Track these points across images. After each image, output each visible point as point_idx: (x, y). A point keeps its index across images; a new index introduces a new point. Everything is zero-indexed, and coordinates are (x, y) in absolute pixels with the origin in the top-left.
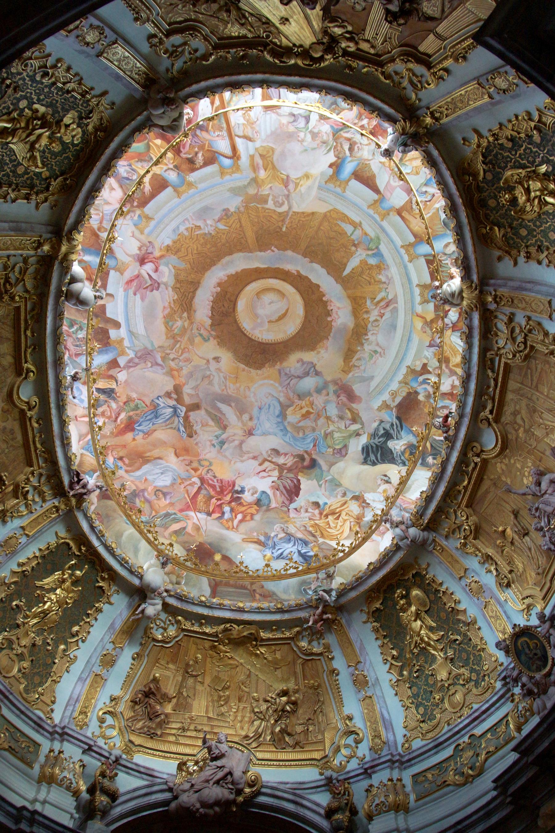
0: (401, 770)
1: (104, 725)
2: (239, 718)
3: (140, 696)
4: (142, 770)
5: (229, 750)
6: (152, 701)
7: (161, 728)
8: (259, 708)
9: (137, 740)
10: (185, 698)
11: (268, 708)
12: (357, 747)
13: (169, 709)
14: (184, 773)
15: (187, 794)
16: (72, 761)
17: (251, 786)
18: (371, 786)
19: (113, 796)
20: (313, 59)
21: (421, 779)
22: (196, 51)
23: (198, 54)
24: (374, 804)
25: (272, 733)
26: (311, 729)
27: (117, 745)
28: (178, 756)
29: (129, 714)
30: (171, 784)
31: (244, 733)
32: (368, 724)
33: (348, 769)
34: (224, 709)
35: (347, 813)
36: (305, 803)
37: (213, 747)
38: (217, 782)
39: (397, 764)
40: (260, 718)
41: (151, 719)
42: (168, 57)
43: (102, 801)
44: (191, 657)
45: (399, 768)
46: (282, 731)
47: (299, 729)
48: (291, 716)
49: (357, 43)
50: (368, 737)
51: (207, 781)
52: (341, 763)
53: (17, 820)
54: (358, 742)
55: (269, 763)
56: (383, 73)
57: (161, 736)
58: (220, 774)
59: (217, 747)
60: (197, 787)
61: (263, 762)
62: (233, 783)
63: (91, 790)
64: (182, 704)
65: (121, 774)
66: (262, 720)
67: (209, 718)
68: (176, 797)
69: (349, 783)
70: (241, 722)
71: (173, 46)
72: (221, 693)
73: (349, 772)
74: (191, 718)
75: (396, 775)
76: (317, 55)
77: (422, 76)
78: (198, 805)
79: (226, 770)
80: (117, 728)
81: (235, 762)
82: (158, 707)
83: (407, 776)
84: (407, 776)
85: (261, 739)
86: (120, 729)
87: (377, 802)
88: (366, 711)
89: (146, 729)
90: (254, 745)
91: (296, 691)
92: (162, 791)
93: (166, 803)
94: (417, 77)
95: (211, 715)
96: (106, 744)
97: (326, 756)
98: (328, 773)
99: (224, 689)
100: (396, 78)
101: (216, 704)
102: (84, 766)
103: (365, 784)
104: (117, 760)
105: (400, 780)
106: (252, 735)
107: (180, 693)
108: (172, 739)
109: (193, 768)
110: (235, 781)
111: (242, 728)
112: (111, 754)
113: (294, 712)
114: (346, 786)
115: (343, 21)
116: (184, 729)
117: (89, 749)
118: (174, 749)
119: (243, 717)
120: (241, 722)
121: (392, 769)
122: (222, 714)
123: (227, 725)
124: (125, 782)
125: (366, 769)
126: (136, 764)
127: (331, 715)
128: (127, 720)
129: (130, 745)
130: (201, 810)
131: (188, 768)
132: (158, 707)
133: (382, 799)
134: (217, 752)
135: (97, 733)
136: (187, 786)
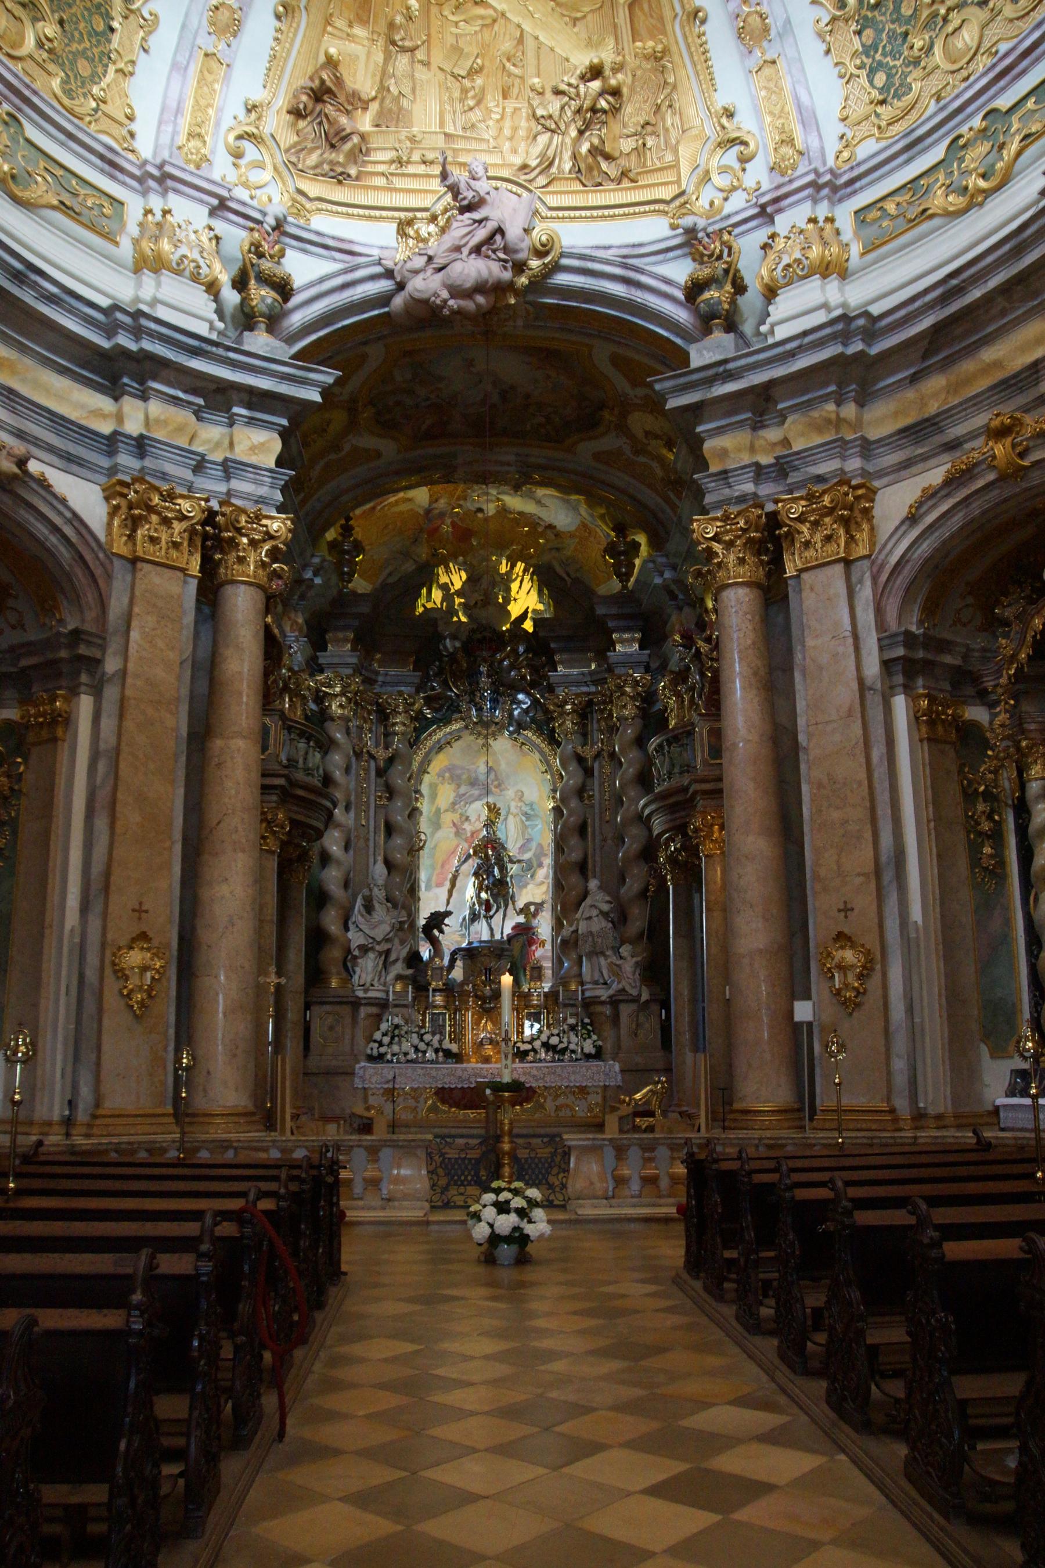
0: (832, 204)
1: (242, 162)
2: (507, 132)
3: (304, 98)
4: (331, 243)
5: (493, 192)
6: (329, 109)
7: (355, 163)
8: (545, 108)
9: (314, 189)
10: (396, 100)
11: (562, 108)
12: (744, 170)
13: (365, 122)
14: (411, 242)
15: (421, 276)
16: (191, 228)
17: (540, 254)
18: (773, 236)
19: (284, 288)
21: (874, 214)
24: (780, 267)
25: (574, 157)
26: (649, 144)
27: (276, 199)
28: (396, 214)
29: (287, 138)
30: (389, 264)
31: (518, 161)
32: (768, 119)
33: (725, 212)
34: (476, 116)
35: (728, 287)
36: (644, 279)
37: (463, 186)
38: (477, 250)
39: (825, 191)
40: (548, 129)
41: (333, 146)
43: (263, 299)
44: (398, 7)
45: (829, 199)
46: (596, 151)
47: (627, 145)
48: (610, 119)
50: (765, 146)
51: (458, 249)
52: (712, 204)
53: (110, 331)
54: (744, 160)
55: (572, 213)
57: (357, 178)
58: (481, 234)
59: (469, 187)
60: (439, 261)
61: (561, 214)
62: (506, 249)
63: (240, 283)
64: (390, 110)
65: (289, 252)
66: (553, 131)
67: (446, 135)
68: (401, 286)
69: (730, 233)
70: (511, 139)
72: (467, 83)
73: (729, 216)
74: (412, 139)
75: (822, 211)
78: (445, 294)
79: (491, 226)
80: (269, 167)
81: (508, 210)
82: (343, 120)
83: (845, 215)
84: (845, 215)
85: (554, 170)
86: (275, 169)
87: (786, 260)
88: (763, 93)
89: (326, 167)
90: (542, 181)
91: (618, 68)
92: (373, 278)
93: (384, 299)
95: (450, 129)
96: (252, 198)
97: (683, 193)
98: (688, 221)
99: (472, 73)
101: (458, 107)
102: (218, 238)
103: (761, 235)
104: (279, 226)
105: (830, 220)
106: (534, 163)
107: (383, 89)
108: (381, 181)
109: (426, 229)
110: (511, 245)
111: (515, 151)
112: (265, 214)
113: (615, 110)
114: (726, 237)
116: (400, 162)
117: (221, 207)
118: (385, 200)
119: (515, 129)
120: (511, 139)
121: (815, 201)
122: (473, 126)
123: (484, 146)
124: (301, 268)
125: (763, 207)
126: (318, 233)
127: (691, 111)
128: (287, 151)
129: (300, 198)
130: (451, 302)
131: (417, 232)
132: (343, 120)
133: (797, 255)
134: (470, 195)
135: (232, 176)
136: (419, 262)
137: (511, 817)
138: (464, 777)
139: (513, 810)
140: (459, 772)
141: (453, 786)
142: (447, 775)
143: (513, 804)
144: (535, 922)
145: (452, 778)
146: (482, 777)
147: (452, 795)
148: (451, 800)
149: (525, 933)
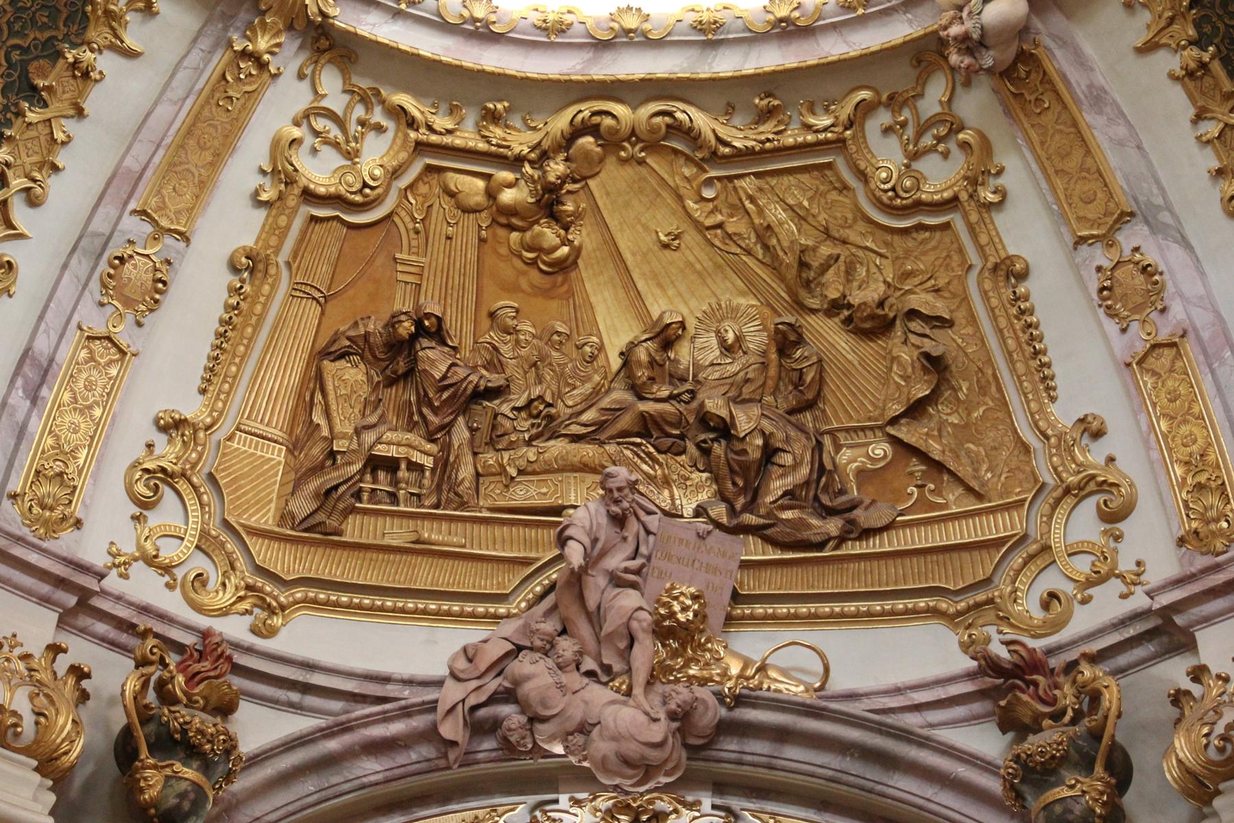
20: (592, 129)
22: (887, 131)
23: (884, 117)
42: (962, 128)
49: (491, 194)
56: (412, 123)
71: (946, 155)
76: (587, 141)
77: (314, 151)
94: (326, 142)
100: (378, 116)
115: (533, 263)
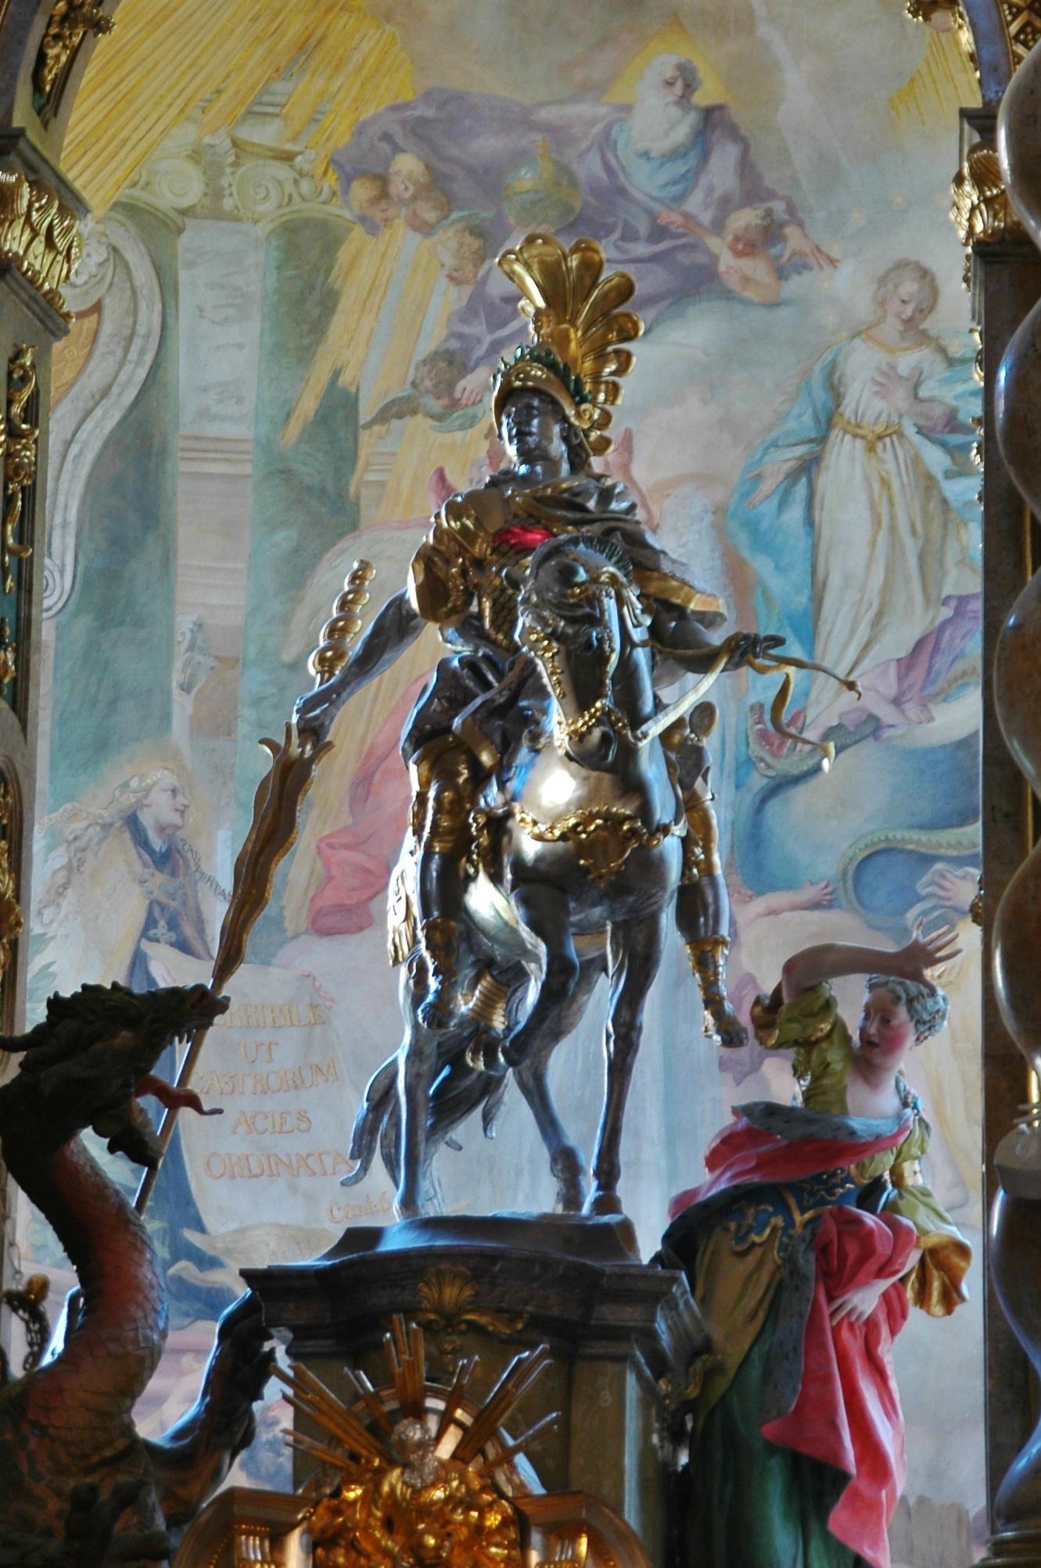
137: (844, 458)
138: (526, 179)
139: (863, 399)
140: (487, 145)
141: (448, 244)
142: (407, 166)
143: (861, 365)
144: (871, 1109)
145: (437, 185)
146: (646, 182)
147: (445, 301)
148: (433, 337)
149: (798, 1184)
